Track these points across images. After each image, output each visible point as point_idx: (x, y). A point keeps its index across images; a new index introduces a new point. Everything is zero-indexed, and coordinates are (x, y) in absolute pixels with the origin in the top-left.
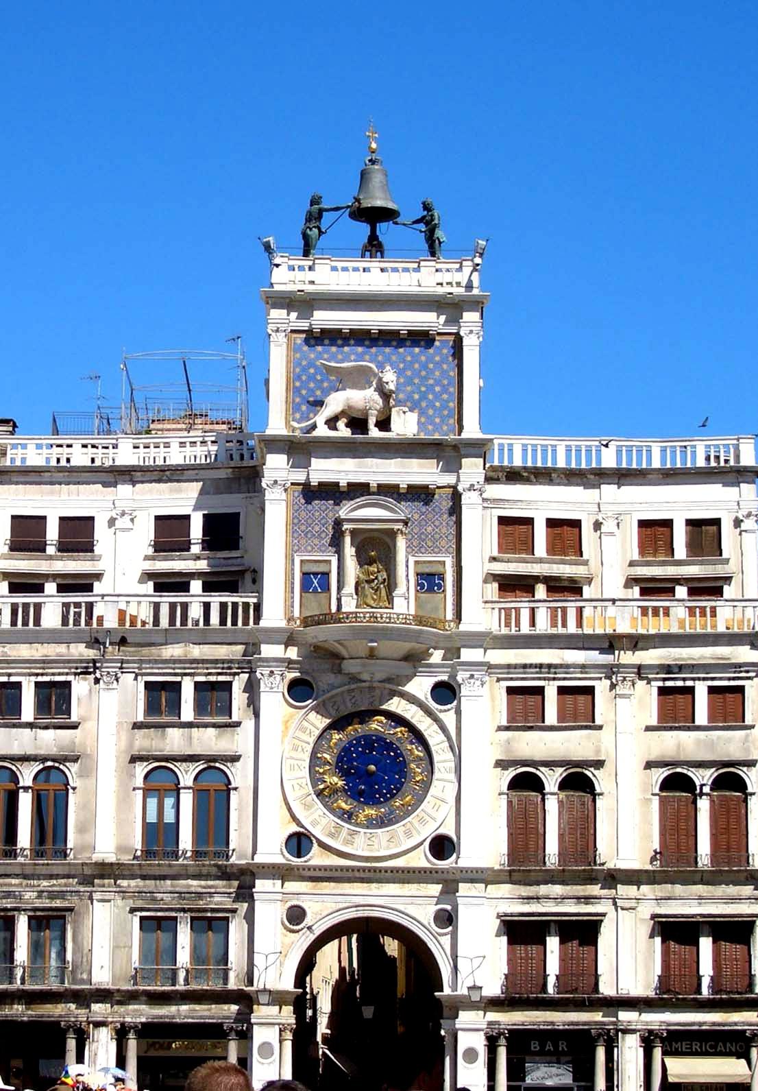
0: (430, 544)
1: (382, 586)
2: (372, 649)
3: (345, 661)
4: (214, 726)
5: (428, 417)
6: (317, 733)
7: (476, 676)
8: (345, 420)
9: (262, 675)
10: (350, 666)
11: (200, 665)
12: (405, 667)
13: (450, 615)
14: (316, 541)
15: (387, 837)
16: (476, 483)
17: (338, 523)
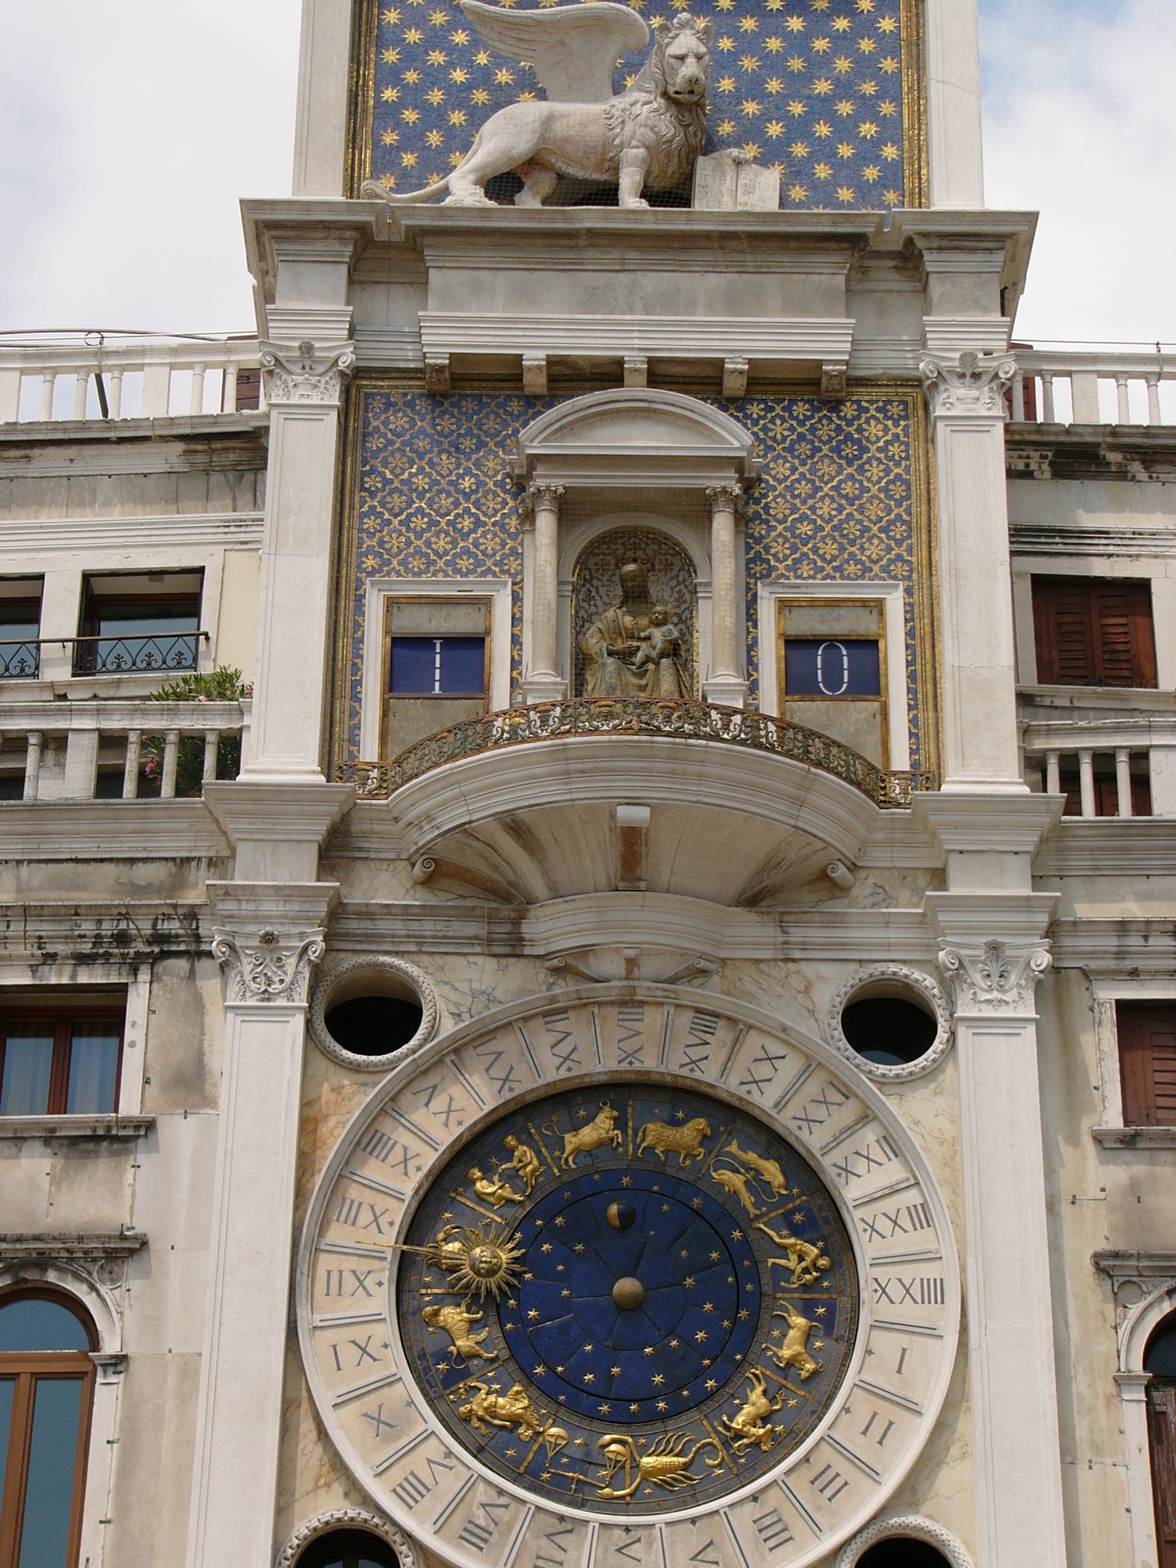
0: (830, 549)
1: (665, 662)
2: (632, 838)
3: (535, 912)
4: (50, 1138)
5: (814, 185)
6: (429, 1159)
7: (1008, 953)
8: (546, 183)
9: (232, 947)
10: (554, 927)
11: (17, 928)
12: (752, 933)
13: (901, 761)
14: (442, 543)
15: (694, 1539)
16: (981, 356)
17: (520, 485)
